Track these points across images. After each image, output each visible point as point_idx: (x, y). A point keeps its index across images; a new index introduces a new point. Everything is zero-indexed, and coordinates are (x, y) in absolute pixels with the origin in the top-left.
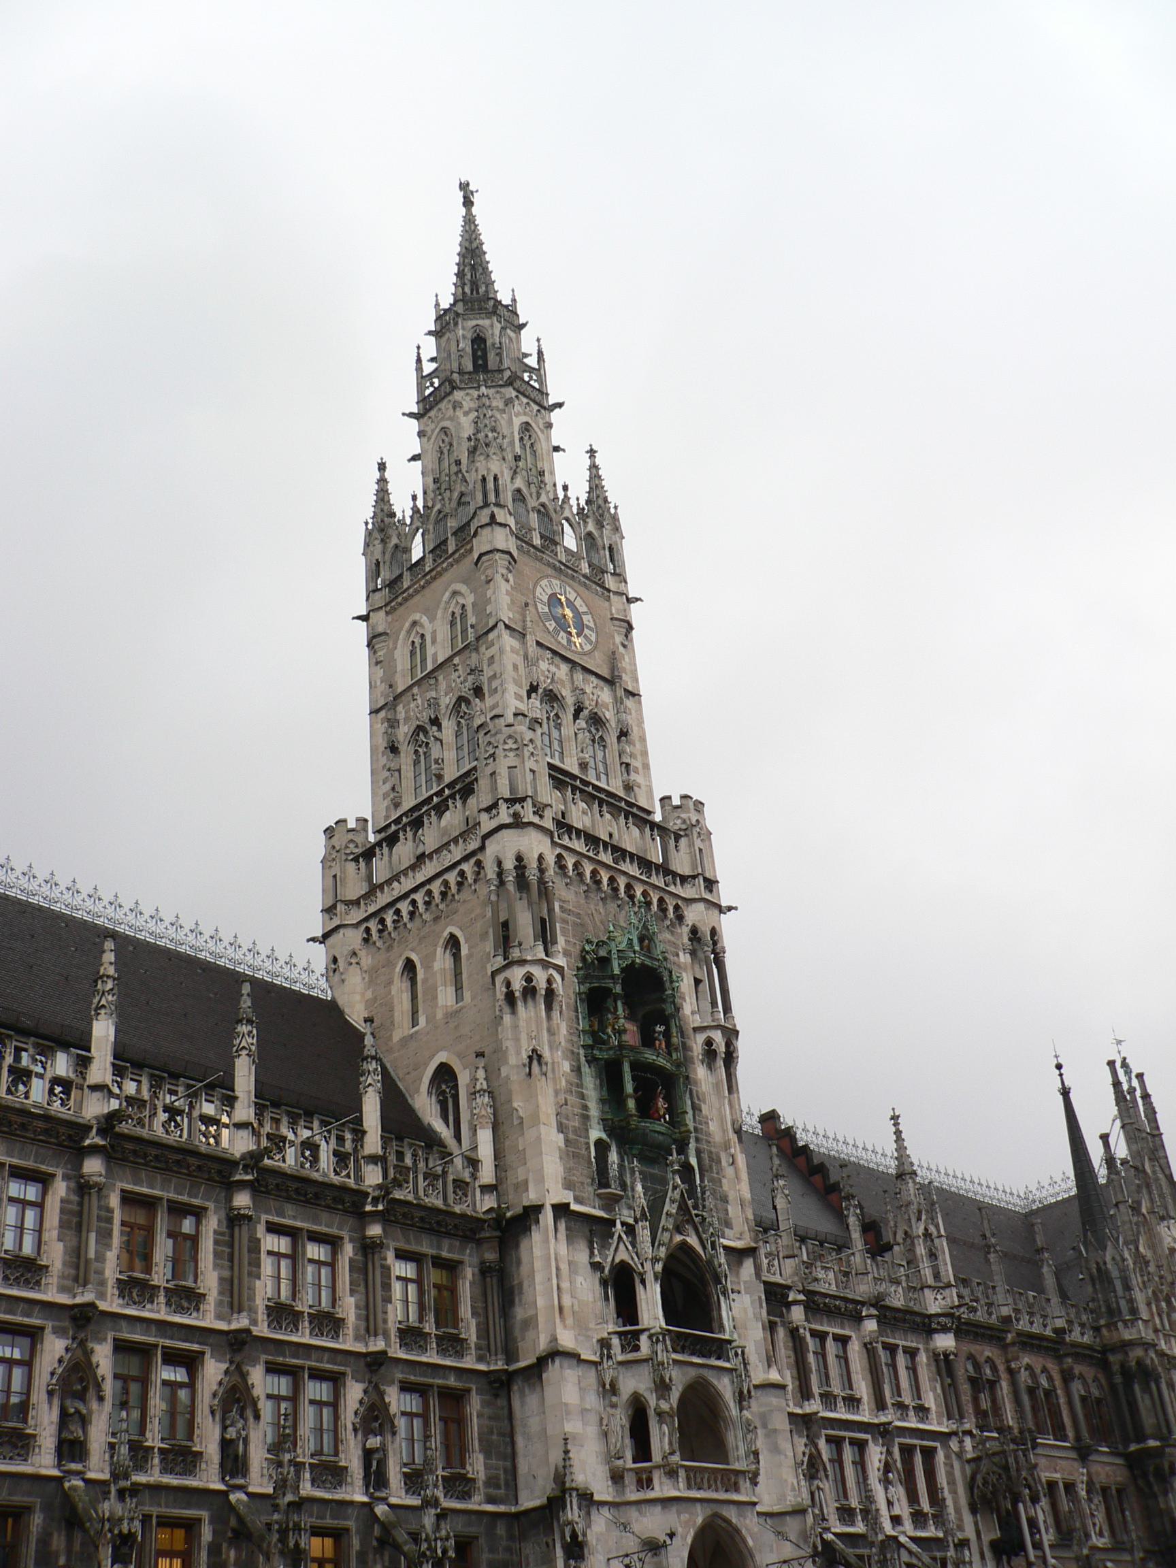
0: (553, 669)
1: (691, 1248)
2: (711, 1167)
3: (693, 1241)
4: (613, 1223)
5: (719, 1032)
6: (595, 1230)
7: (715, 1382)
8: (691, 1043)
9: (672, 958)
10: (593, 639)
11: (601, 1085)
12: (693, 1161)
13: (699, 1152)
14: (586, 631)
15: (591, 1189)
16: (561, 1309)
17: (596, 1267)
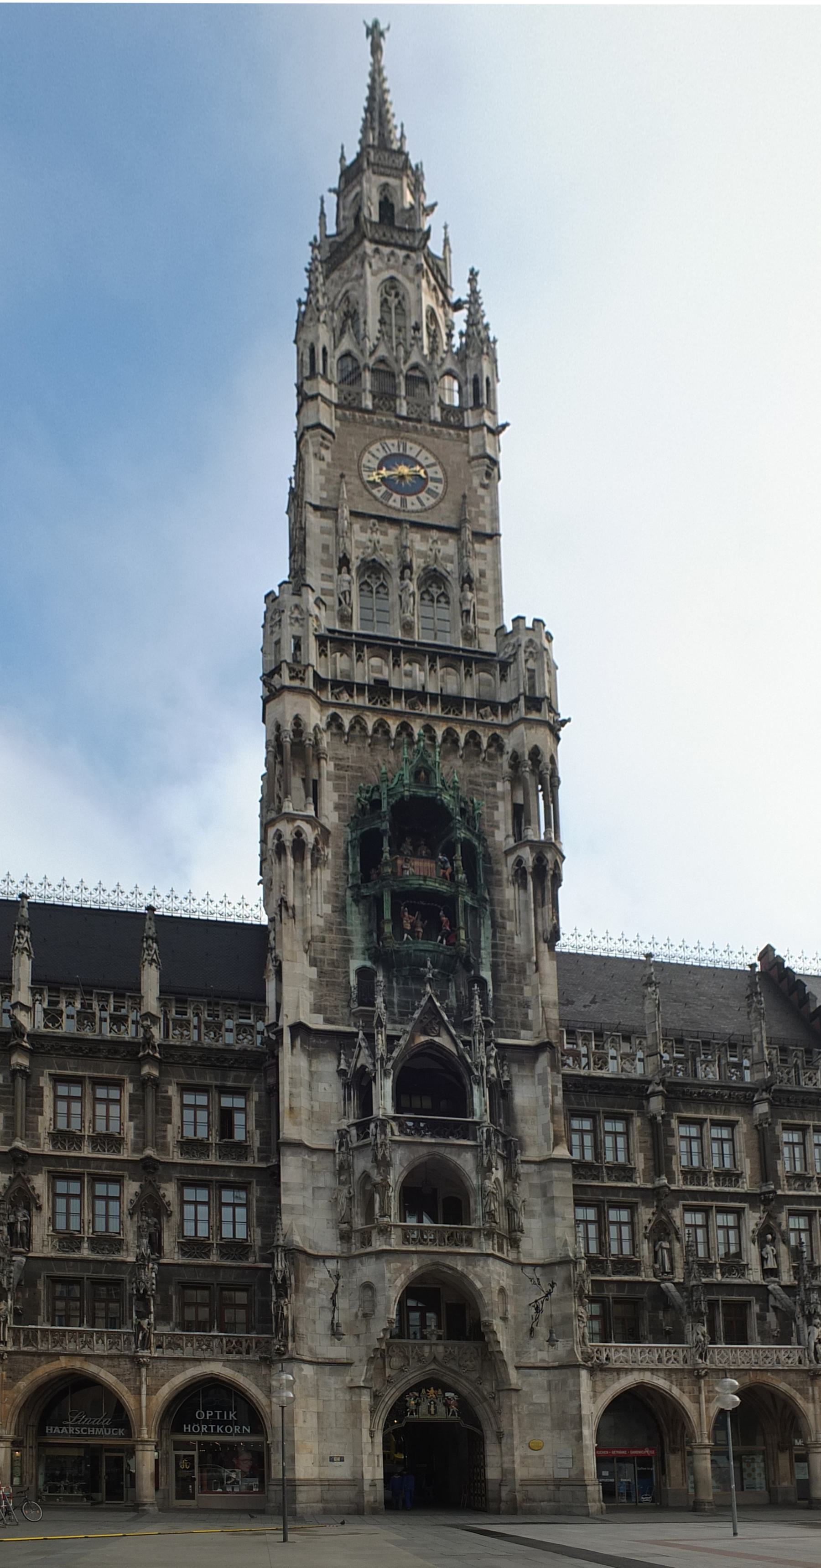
0: (377, 536)
1: (440, 1047)
2: (510, 978)
3: (443, 1040)
4: (357, 1034)
5: (528, 849)
6: (341, 1042)
7: (454, 1158)
8: (497, 867)
9: (485, 790)
10: (440, 488)
11: (370, 920)
12: (486, 974)
13: (495, 968)
14: (431, 485)
15: (346, 1010)
16: (291, 1109)
17: (341, 1073)
